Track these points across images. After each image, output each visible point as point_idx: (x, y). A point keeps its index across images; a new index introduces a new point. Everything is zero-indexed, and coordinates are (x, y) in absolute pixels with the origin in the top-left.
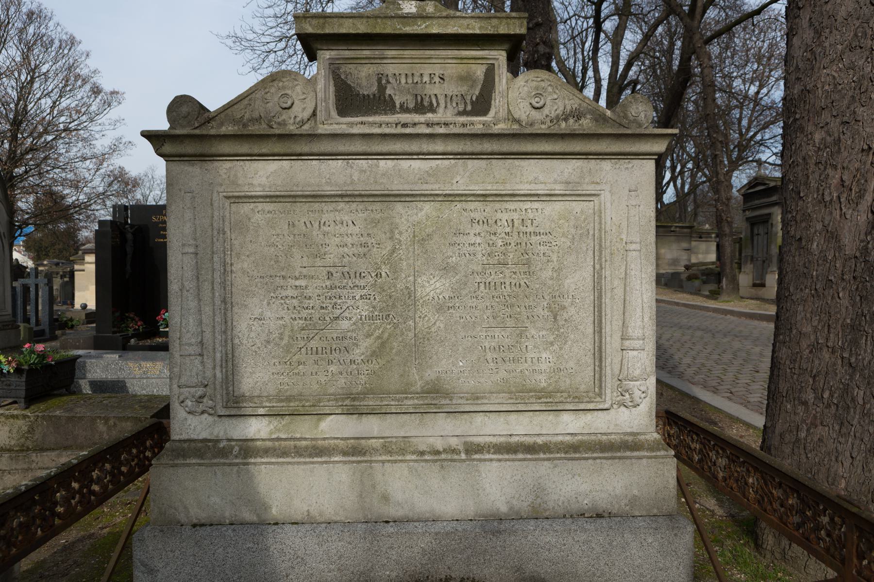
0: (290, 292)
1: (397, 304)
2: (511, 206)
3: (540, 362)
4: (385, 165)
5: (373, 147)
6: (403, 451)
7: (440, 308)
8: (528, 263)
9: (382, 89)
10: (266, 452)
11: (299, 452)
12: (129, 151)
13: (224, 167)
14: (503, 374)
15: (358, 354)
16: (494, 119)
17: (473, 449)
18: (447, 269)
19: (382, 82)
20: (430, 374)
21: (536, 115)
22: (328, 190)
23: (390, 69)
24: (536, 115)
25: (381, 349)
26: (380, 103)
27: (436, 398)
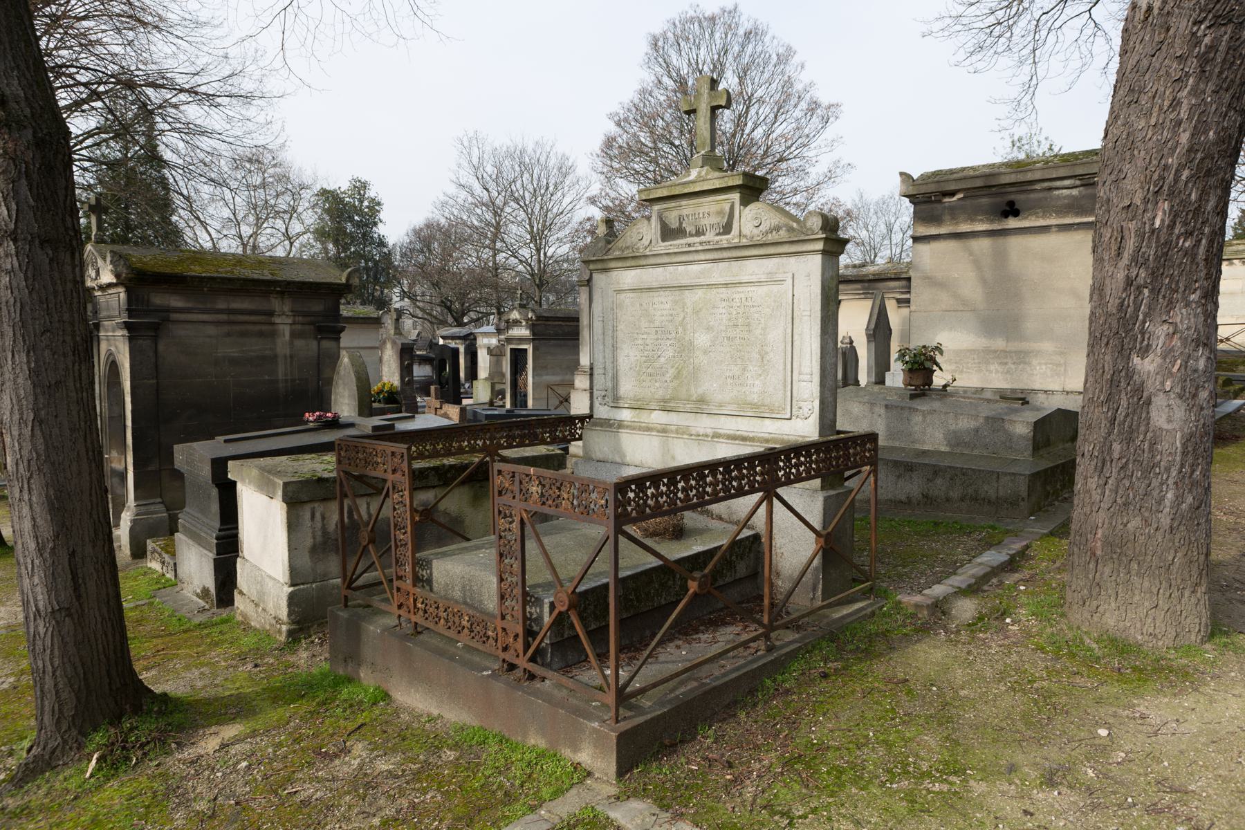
0: (640, 342)
1: (686, 348)
2: (740, 289)
3: (755, 387)
4: (681, 268)
5: (673, 259)
6: (683, 433)
7: (705, 352)
8: (749, 325)
9: (681, 224)
10: (628, 427)
11: (640, 429)
12: (846, 176)
13: (614, 274)
14: (735, 392)
15: (668, 377)
16: (733, 238)
17: (716, 435)
18: (709, 329)
19: (681, 219)
20: (700, 391)
21: (756, 231)
22: (655, 285)
23: (685, 212)
24: (756, 231)
25: (677, 377)
26: (679, 233)
27: (701, 406)
